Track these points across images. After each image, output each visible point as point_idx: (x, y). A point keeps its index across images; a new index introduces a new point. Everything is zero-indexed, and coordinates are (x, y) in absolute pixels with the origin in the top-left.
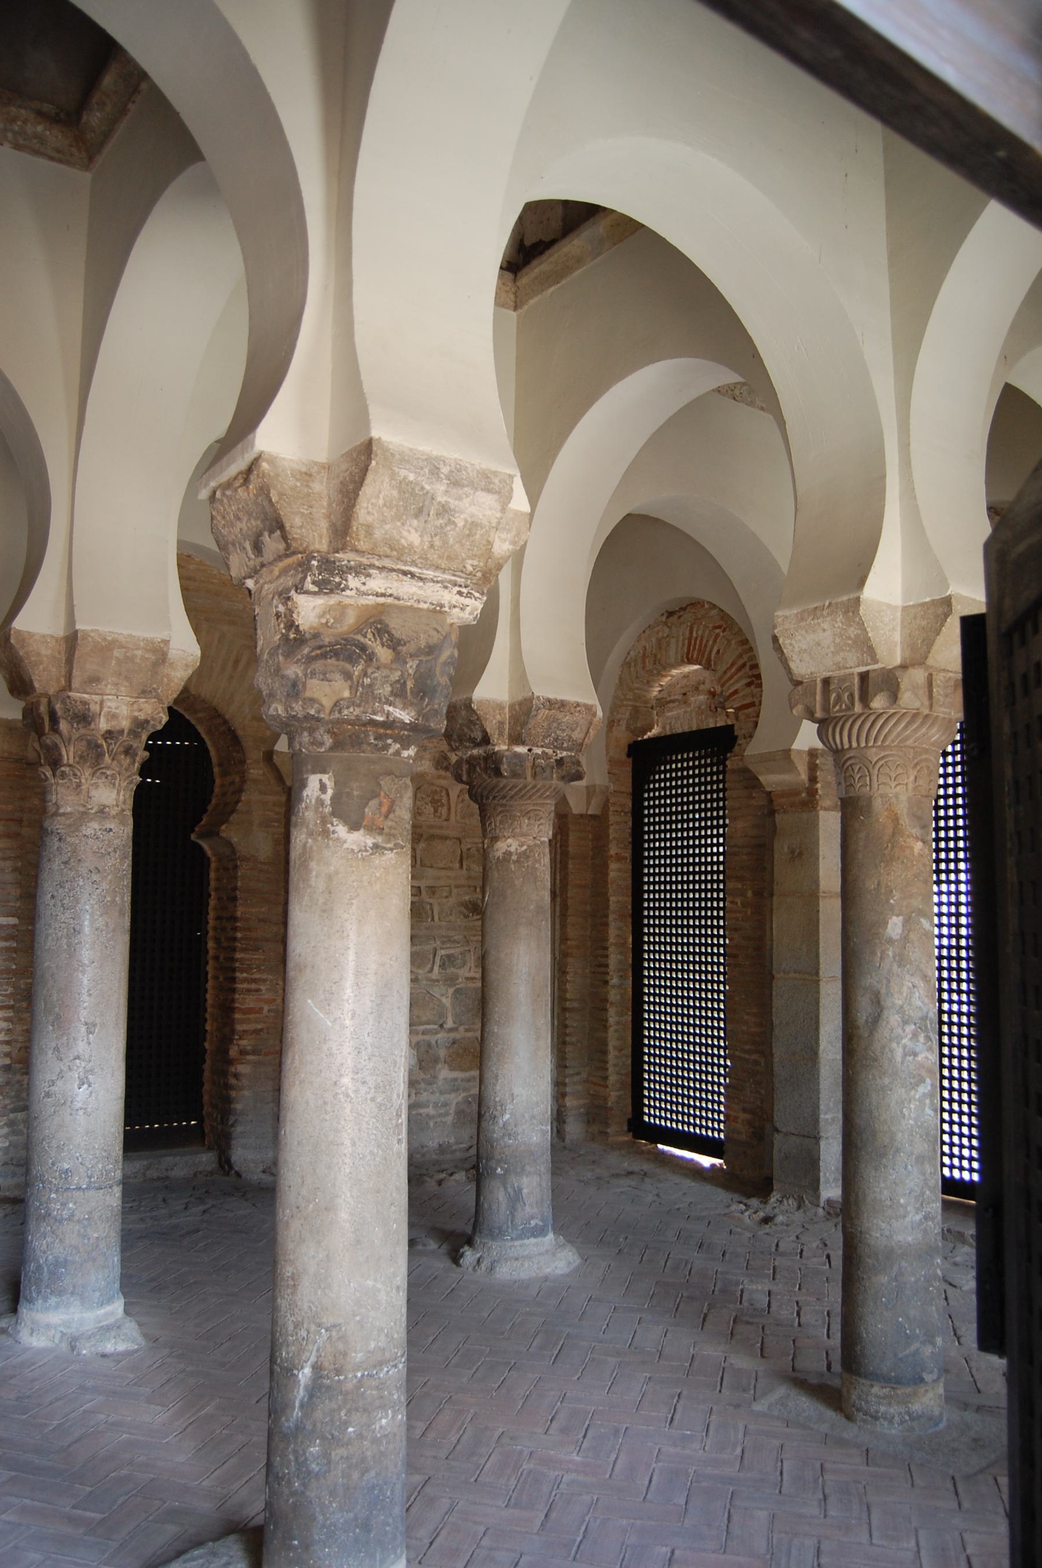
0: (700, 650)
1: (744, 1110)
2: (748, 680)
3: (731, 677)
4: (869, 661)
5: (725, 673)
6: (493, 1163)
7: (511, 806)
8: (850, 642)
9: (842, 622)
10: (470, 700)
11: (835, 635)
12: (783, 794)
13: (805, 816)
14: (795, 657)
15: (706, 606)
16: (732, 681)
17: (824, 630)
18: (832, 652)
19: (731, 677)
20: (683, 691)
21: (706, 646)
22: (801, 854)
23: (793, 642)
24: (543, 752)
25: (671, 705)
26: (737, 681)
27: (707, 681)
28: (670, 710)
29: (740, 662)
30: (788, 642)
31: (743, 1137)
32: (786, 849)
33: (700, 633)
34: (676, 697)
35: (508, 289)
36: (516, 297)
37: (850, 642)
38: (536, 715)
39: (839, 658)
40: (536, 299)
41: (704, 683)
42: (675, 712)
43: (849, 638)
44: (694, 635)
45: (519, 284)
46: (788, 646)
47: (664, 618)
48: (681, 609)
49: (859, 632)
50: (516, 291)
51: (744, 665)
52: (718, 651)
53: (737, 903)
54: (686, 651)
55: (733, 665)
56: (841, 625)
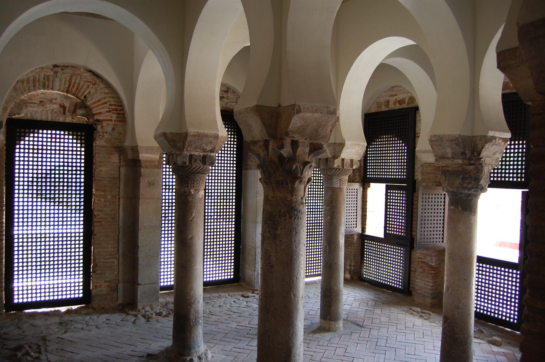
0: (77, 89)
1: (105, 282)
2: (108, 110)
3: (97, 106)
5: (94, 103)
6: (198, 320)
12: (146, 161)
13: (156, 170)
15: (82, 70)
16: (98, 108)
19: (97, 106)
20: (41, 100)
21: (81, 88)
22: (153, 184)
25: (33, 105)
26: (103, 108)
27: (59, 99)
28: (33, 107)
29: (104, 101)
31: (105, 292)
32: (146, 182)
33: (78, 81)
34: (36, 102)
41: (56, 100)
42: (35, 109)
44: (73, 81)
47: (52, 67)
48: (64, 66)
51: (106, 103)
52: (89, 93)
53: (102, 201)
54: (67, 86)
55: (99, 101)
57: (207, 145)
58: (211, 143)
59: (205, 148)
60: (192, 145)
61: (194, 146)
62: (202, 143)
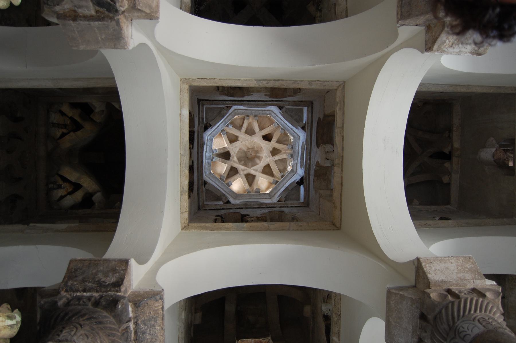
4: (479, 278)
7: (98, 334)
8: (467, 269)
9: (462, 261)
10: (130, 259)
11: (458, 265)
14: (431, 272)
17: (451, 263)
18: (456, 272)
23: (431, 265)
24: (132, 330)
30: (427, 265)
35: (186, 222)
36: (184, 227)
37: (467, 269)
38: (157, 301)
39: (461, 275)
40: (196, 230)
43: (467, 268)
45: (190, 224)
46: (428, 268)
49: (472, 266)
50: (186, 226)
56: (462, 262)
57: (106, 275)
58: (114, 271)
59: (103, 280)
60: (76, 277)
61: (80, 278)
62: (98, 271)
